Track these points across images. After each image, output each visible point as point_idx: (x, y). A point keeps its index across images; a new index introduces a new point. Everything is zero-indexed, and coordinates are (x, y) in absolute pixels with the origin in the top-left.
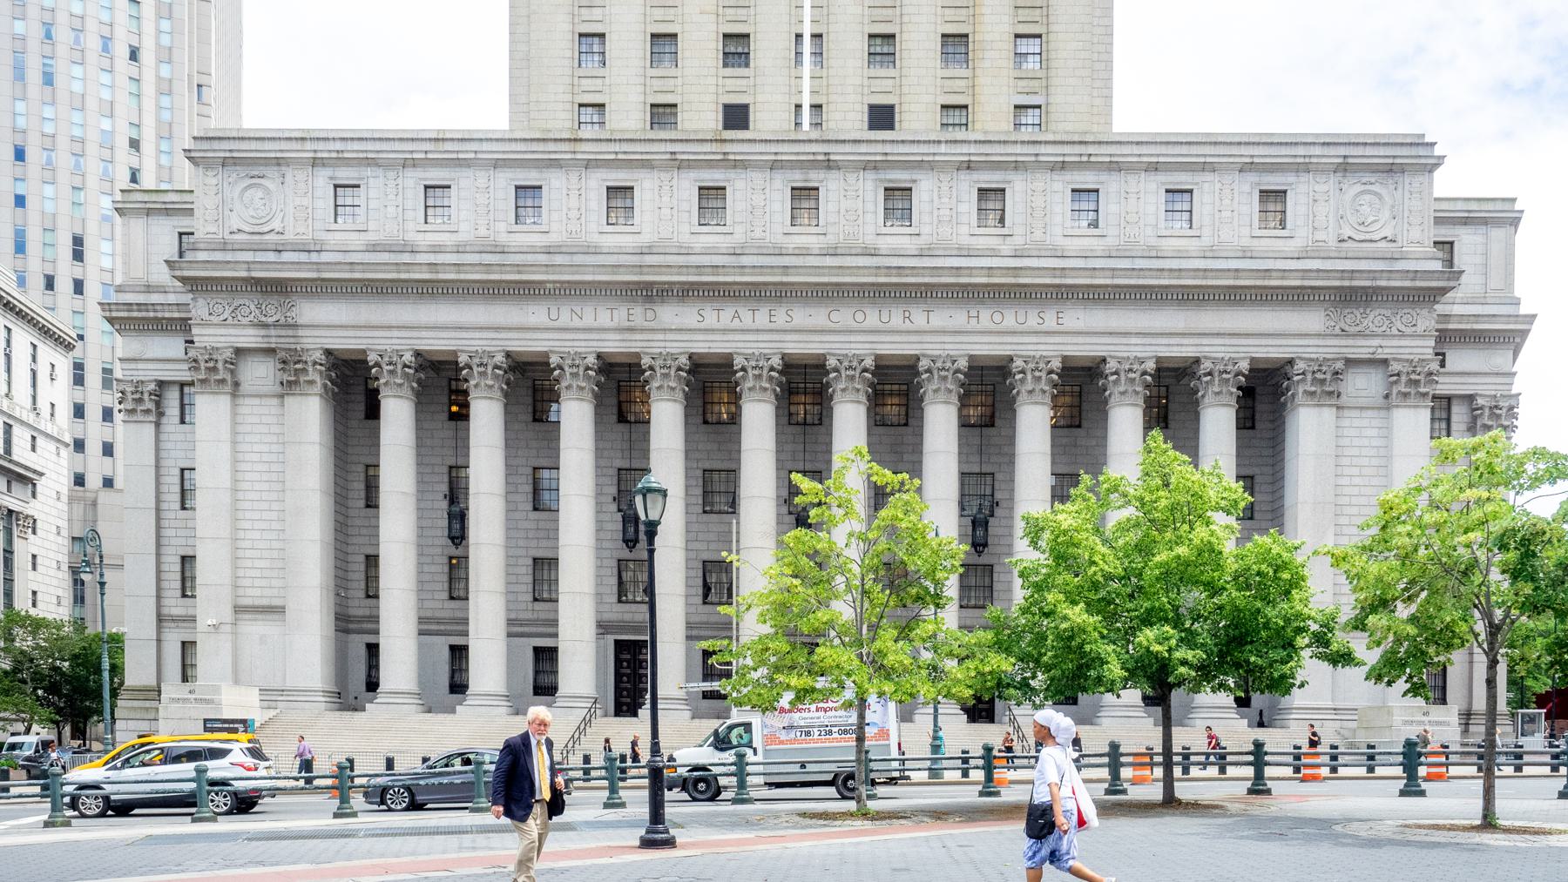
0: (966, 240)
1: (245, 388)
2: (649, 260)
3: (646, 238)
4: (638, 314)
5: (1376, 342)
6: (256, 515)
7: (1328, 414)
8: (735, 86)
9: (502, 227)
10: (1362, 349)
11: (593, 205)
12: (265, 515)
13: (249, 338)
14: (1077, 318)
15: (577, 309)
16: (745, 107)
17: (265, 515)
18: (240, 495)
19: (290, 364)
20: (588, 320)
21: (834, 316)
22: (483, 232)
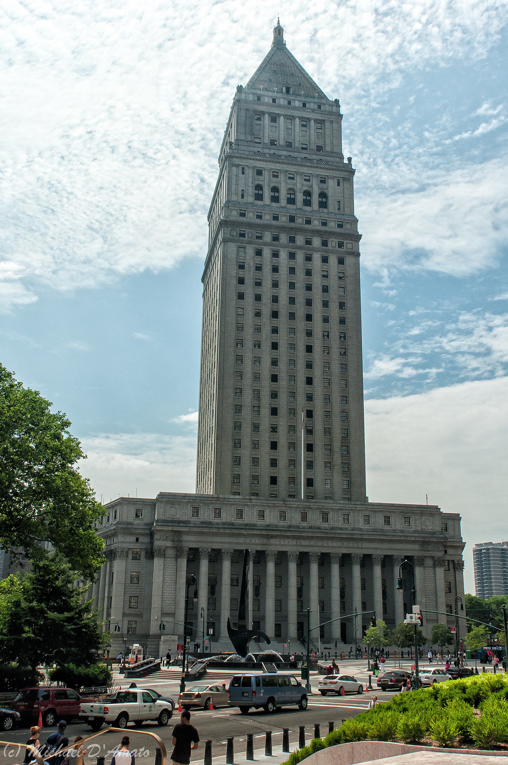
0: (340, 526)
1: (167, 556)
2: (268, 528)
3: (267, 523)
4: (265, 541)
5: (431, 553)
6: (168, 589)
7: (422, 569)
8: (274, 472)
9: (233, 519)
10: (428, 554)
11: (255, 515)
12: (170, 589)
13: (169, 544)
14: (366, 545)
15: (251, 539)
16: (276, 477)
17: (170, 589)
18: (164, 584)
19: (179, 552)
20: (253, 541)
21: (311, 543)
22: (229, 520)
